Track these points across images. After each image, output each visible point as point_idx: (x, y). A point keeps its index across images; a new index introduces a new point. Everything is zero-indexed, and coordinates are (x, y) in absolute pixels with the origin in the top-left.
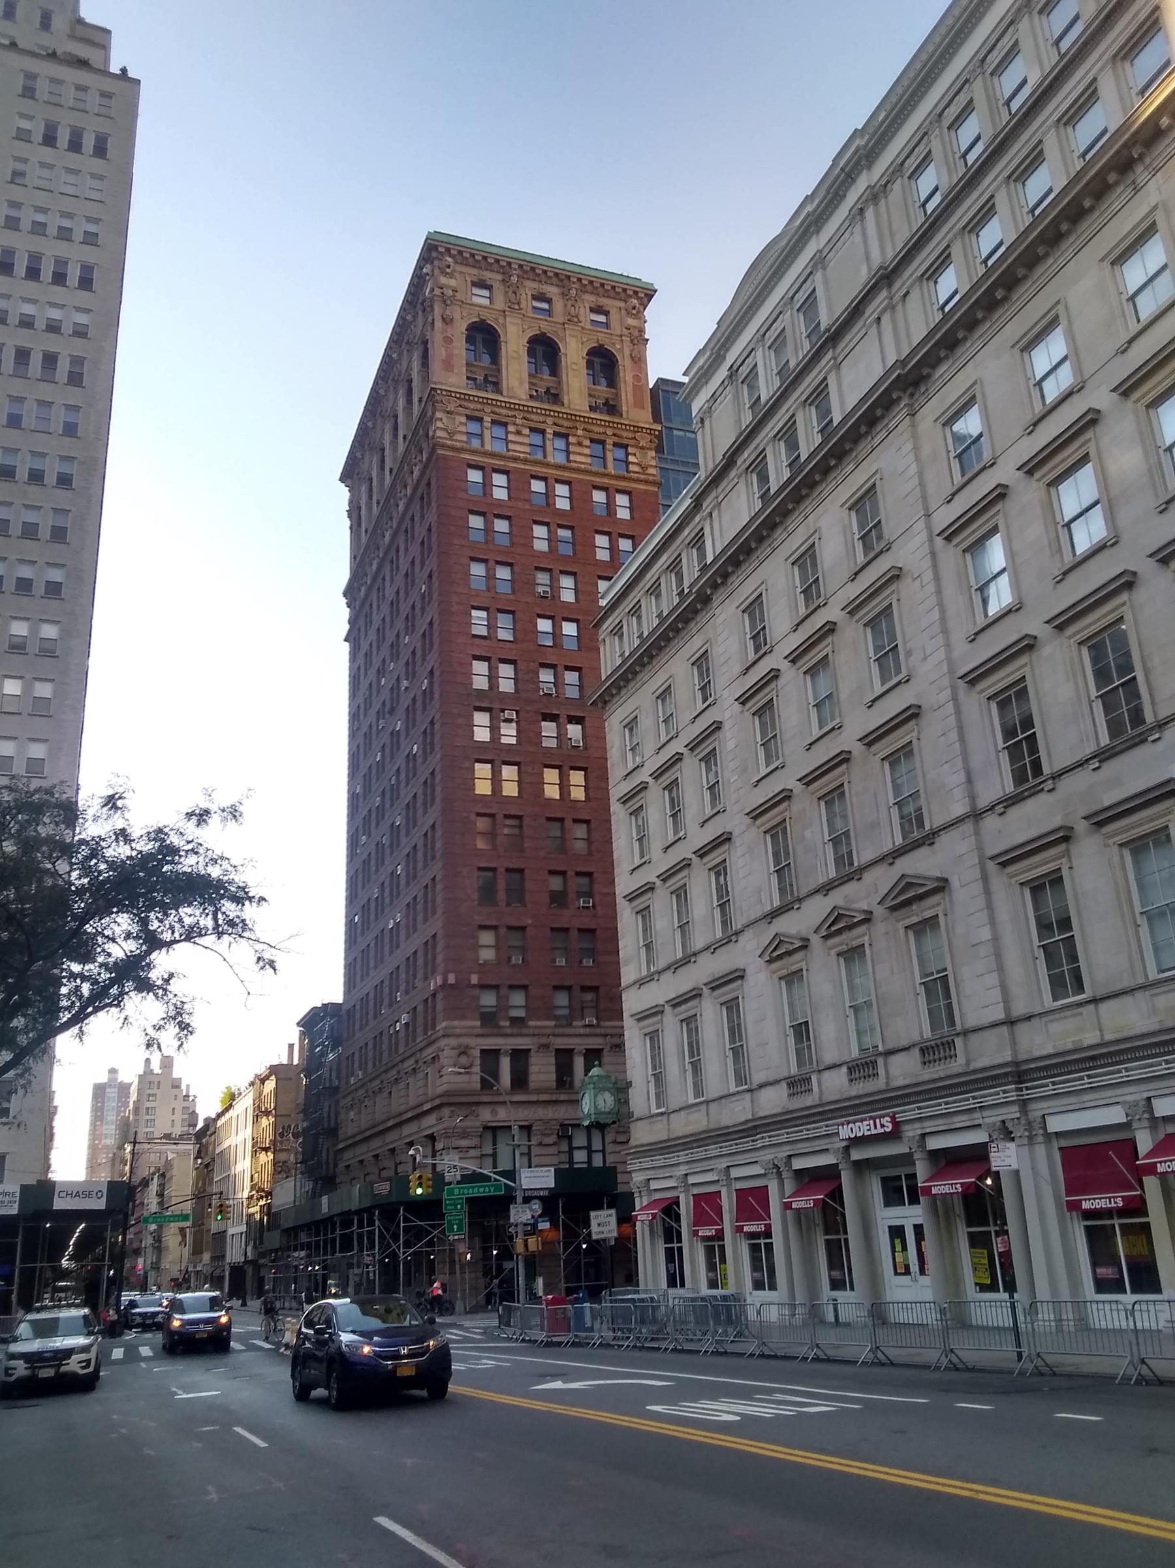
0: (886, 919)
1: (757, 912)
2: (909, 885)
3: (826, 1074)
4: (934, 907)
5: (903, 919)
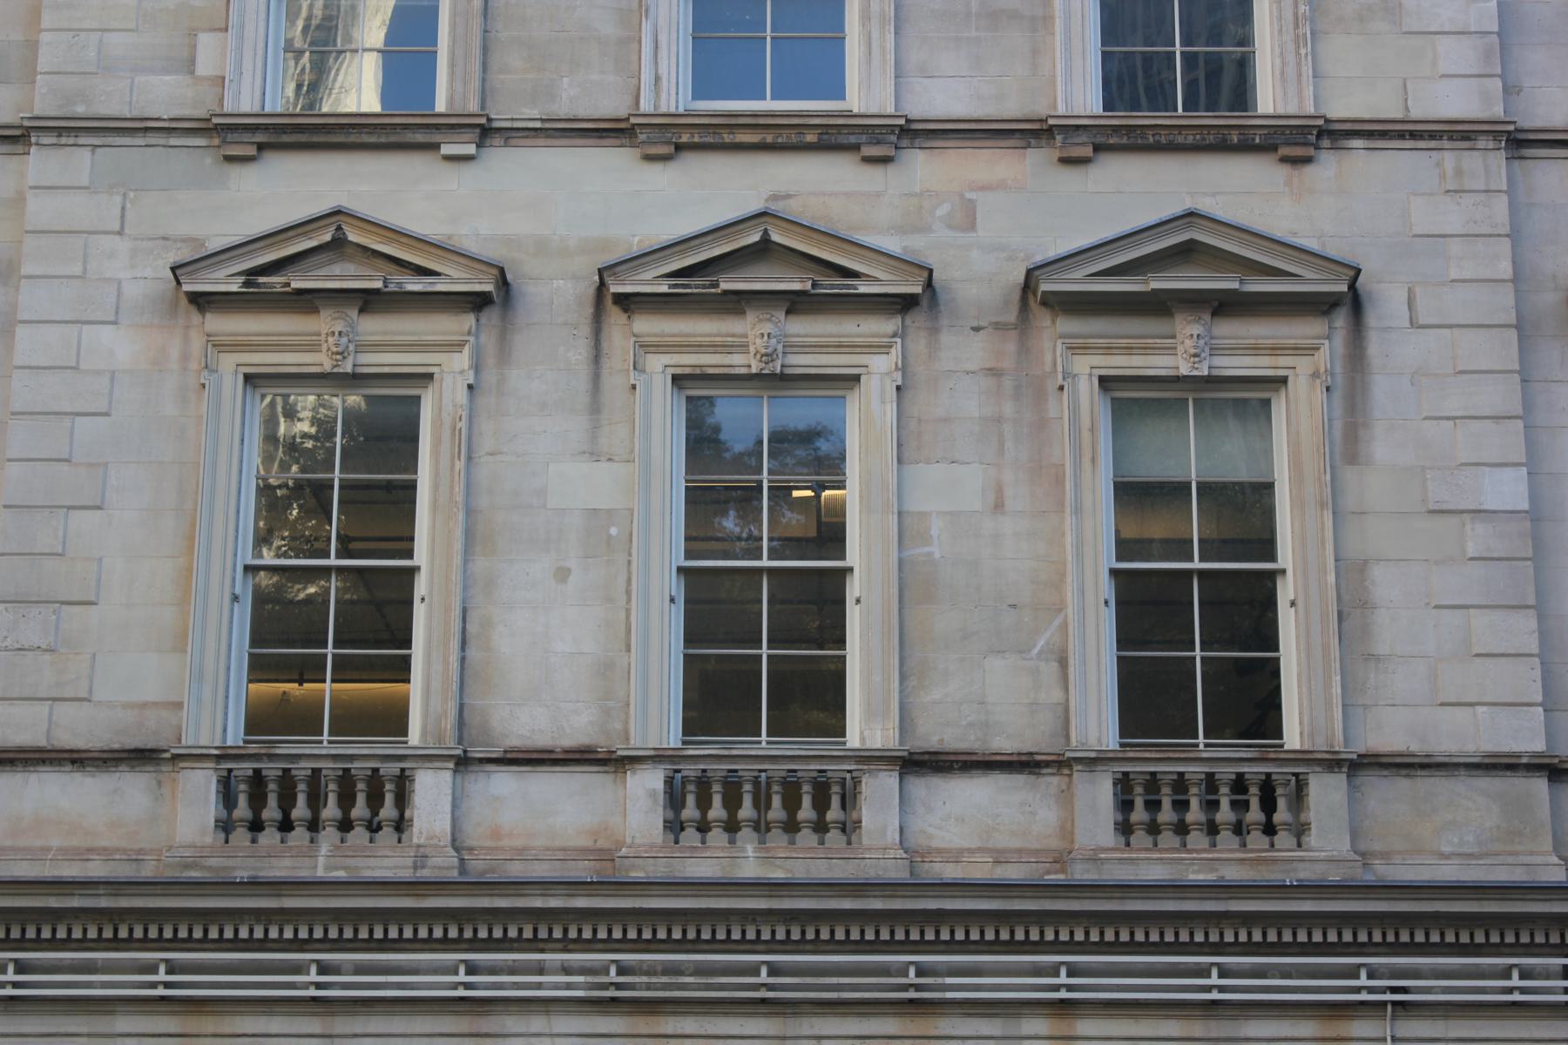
0: (998, 326)
1: (165, 95)
2: (1187, 253)
3: (504, 782)
4: (1275, 350)
5: (1108, 350)
